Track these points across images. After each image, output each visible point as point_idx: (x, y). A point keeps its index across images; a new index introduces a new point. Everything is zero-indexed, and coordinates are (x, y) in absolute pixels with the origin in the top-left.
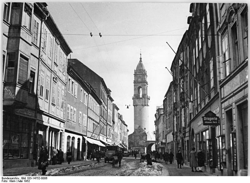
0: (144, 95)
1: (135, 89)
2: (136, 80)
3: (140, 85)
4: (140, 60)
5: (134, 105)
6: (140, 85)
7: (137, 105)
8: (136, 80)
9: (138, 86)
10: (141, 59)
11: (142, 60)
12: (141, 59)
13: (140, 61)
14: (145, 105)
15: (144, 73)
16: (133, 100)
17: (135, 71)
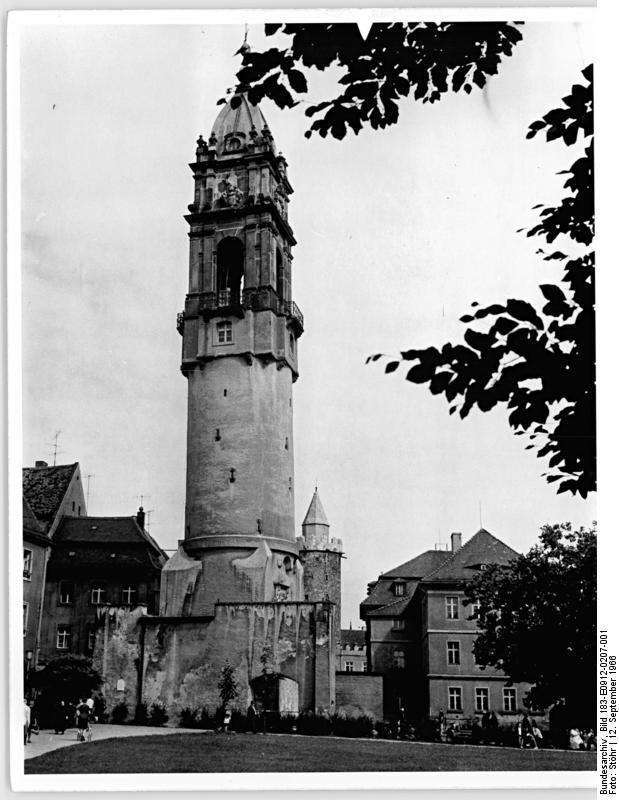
5: (187, 369)
7: (206, 361)
9: (220, 238)
14: (265, 359)
17: (200, 142)
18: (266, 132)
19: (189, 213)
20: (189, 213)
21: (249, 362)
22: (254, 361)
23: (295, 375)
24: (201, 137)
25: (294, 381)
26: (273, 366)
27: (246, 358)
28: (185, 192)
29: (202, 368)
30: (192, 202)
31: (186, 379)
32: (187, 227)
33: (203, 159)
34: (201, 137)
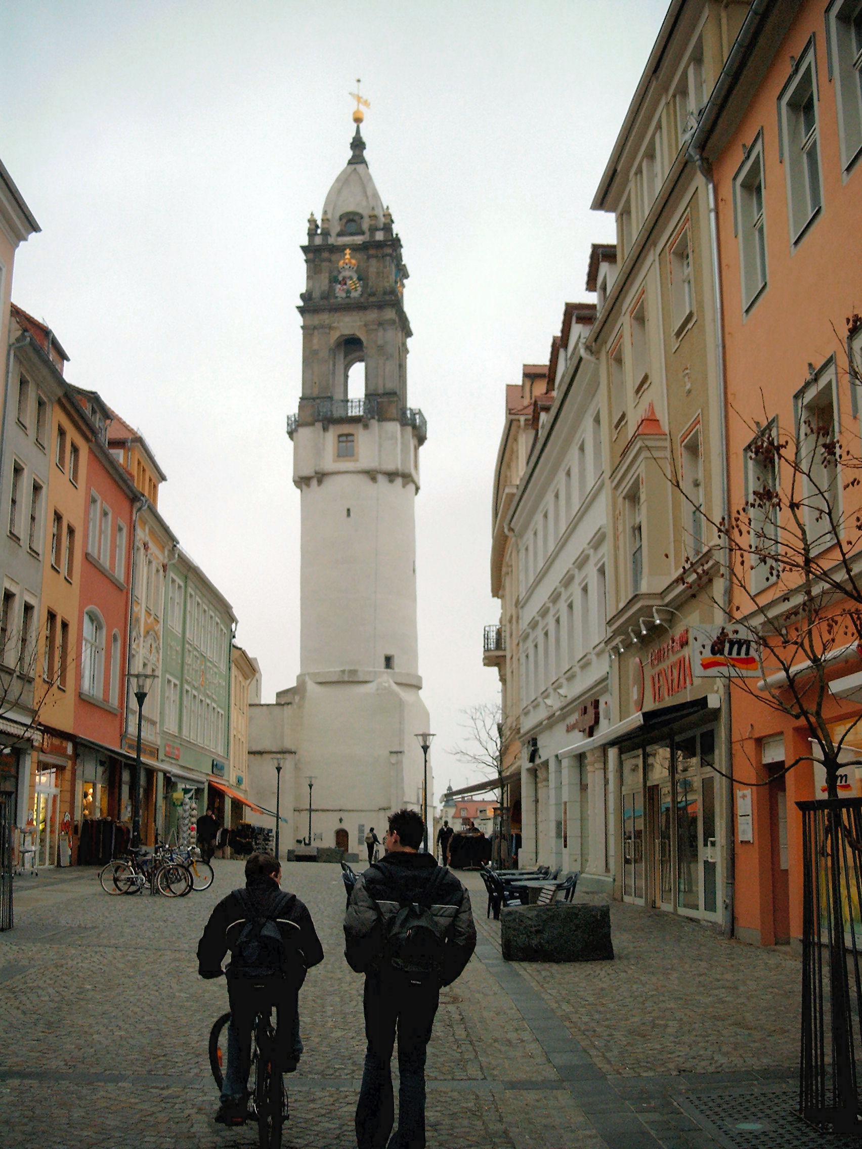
0: (388, 402)
1: (310, 358)
2: (316, 295)
3: (349, 324)
4: (349, 154)
5: (302, 481)
6: (349, 324)
7: (321, 477)
8: (316, 295)
9: (335, 336)
10: (358, 145)
11: (367, 154)
12: (358, 145)
13: (350, 163)
15: (380, 236)
16: (290, 444)
17: (312, 221)
18: (388, 216)
19: (301, 304)
20: (301, 304)
21: (374, 480)
22: (380, 478)
23: (417, 489)
24: (312, 215)
25: (416, 494)
26: (399, 481)
27: (372, 475)
28: (295, 277)
29: (320, 482)
30: (304, 291)
31: (299, 491)
32: (298, 320)
33: (318, 241)
34: (312, 215)
